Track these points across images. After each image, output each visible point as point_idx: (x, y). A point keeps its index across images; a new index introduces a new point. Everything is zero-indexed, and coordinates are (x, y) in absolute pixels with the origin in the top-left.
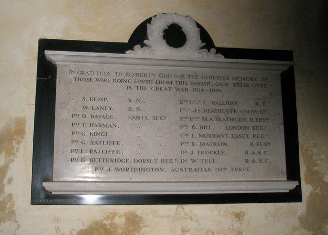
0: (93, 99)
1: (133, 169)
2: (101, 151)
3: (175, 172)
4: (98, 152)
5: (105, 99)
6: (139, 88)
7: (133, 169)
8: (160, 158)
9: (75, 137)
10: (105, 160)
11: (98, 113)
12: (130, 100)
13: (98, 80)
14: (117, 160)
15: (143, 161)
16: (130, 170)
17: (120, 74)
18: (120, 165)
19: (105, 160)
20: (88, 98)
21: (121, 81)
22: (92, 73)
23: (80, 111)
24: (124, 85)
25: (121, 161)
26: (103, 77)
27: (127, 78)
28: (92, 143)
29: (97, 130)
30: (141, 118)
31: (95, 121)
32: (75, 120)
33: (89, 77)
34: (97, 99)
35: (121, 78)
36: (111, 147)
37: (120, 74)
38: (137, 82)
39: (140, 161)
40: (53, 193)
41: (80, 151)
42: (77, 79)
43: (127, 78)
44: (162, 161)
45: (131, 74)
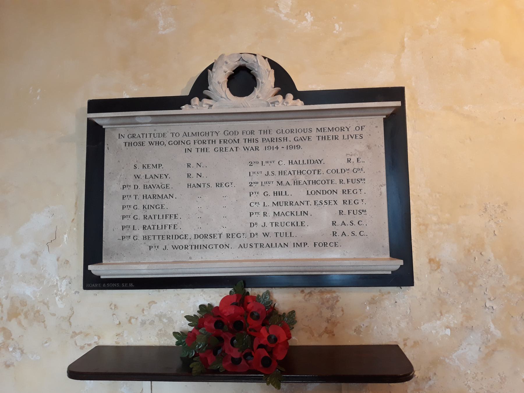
0: (146, 166)
1: (193, 247)
2: (156, 227)
3: (244, 249)
4: (152, 227)
5: (160, 165)
6: (199, 150)
7: (193, 247)
8: (225, 232)
9: (126, 212)
10: (161, 237)
11: (151, 182)
12: (189, 165)
13: (151, 143)
14: (174, 237)
15: (205, 236)
16: (189, 247)
17: (177, 135)
18: (178, 242)
19: (161, 237)
20: (140, 166)
21: (178, 143)
22: (145, 135)
23: (131, 182)
24: (182, 147)
25: (179, 237)
26: (157, 139)
27: (186, 139)
28: (145, 217)
29: (151, 202)
30: (202, 185)
31: (149, 192)
32: (126, 192)
33: (141, 140)
34: (151, 166)
35: (178, 139)
36: (168, 222)
37: (177, 135)
38: (197, 143)
39: (201, 236)
40: (102, 277)
41: (132, 227)
42: (127, 144)
43: (186, 139)
44: (228, 236)
45: (190, 134)
